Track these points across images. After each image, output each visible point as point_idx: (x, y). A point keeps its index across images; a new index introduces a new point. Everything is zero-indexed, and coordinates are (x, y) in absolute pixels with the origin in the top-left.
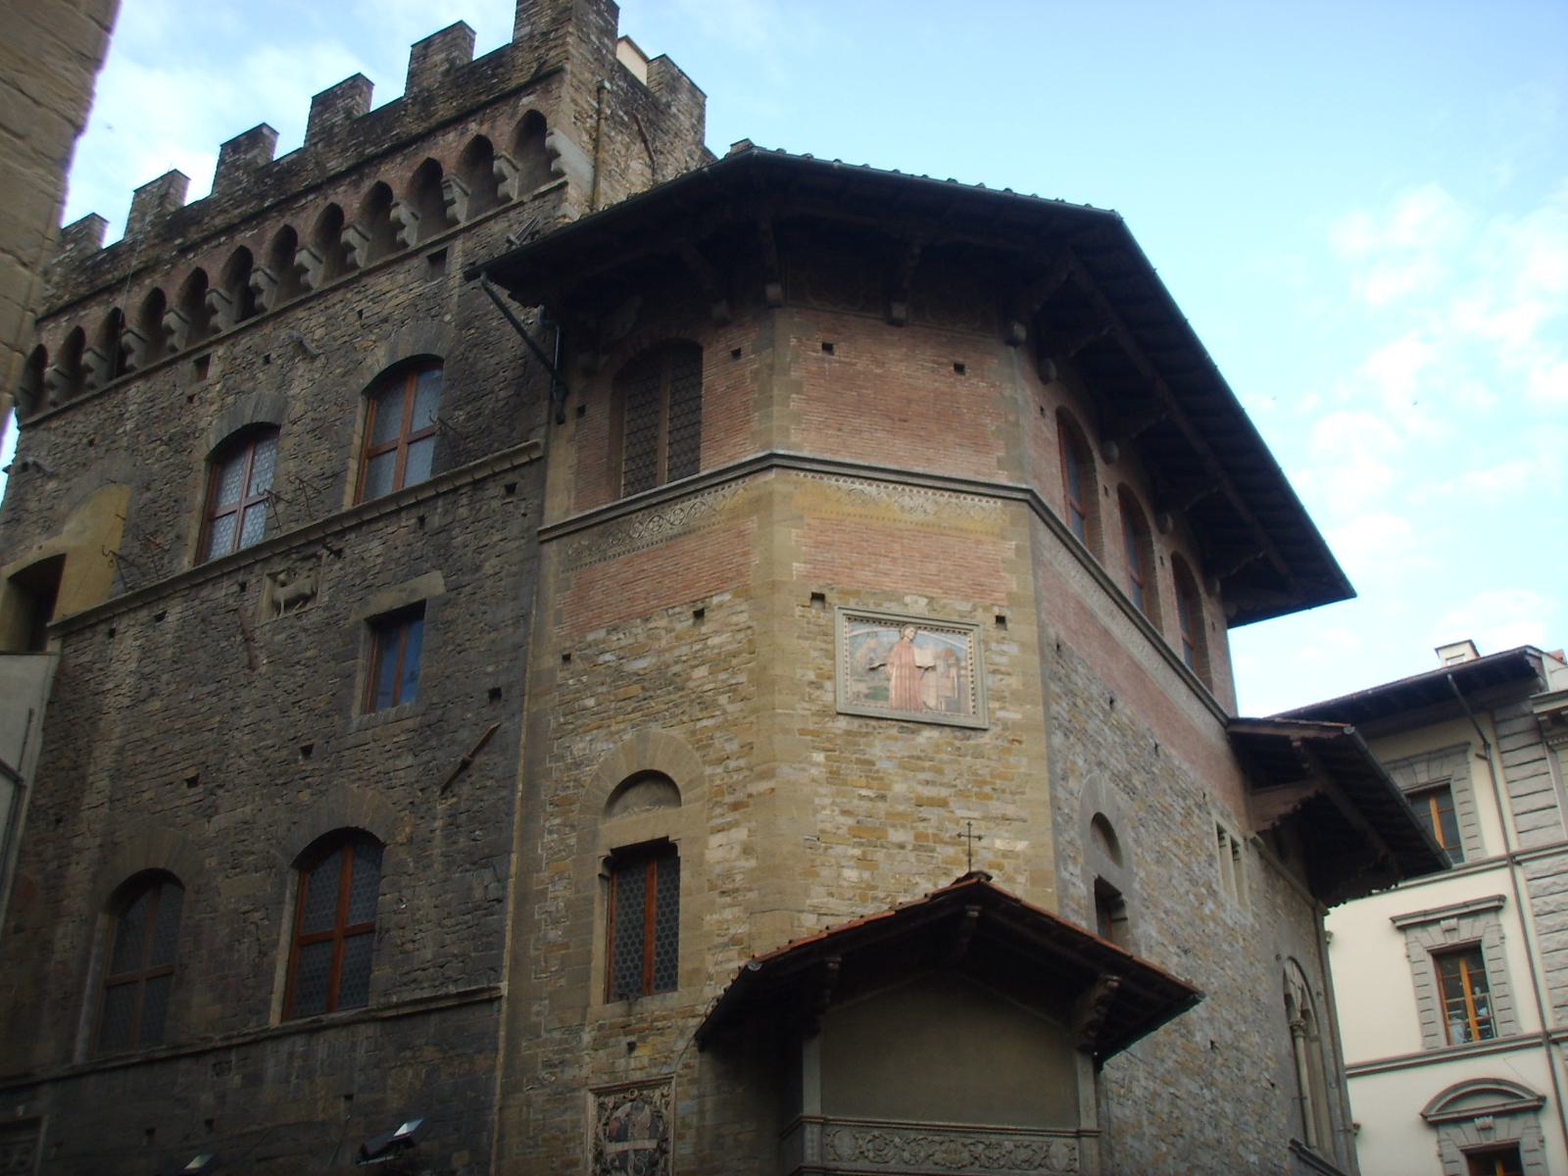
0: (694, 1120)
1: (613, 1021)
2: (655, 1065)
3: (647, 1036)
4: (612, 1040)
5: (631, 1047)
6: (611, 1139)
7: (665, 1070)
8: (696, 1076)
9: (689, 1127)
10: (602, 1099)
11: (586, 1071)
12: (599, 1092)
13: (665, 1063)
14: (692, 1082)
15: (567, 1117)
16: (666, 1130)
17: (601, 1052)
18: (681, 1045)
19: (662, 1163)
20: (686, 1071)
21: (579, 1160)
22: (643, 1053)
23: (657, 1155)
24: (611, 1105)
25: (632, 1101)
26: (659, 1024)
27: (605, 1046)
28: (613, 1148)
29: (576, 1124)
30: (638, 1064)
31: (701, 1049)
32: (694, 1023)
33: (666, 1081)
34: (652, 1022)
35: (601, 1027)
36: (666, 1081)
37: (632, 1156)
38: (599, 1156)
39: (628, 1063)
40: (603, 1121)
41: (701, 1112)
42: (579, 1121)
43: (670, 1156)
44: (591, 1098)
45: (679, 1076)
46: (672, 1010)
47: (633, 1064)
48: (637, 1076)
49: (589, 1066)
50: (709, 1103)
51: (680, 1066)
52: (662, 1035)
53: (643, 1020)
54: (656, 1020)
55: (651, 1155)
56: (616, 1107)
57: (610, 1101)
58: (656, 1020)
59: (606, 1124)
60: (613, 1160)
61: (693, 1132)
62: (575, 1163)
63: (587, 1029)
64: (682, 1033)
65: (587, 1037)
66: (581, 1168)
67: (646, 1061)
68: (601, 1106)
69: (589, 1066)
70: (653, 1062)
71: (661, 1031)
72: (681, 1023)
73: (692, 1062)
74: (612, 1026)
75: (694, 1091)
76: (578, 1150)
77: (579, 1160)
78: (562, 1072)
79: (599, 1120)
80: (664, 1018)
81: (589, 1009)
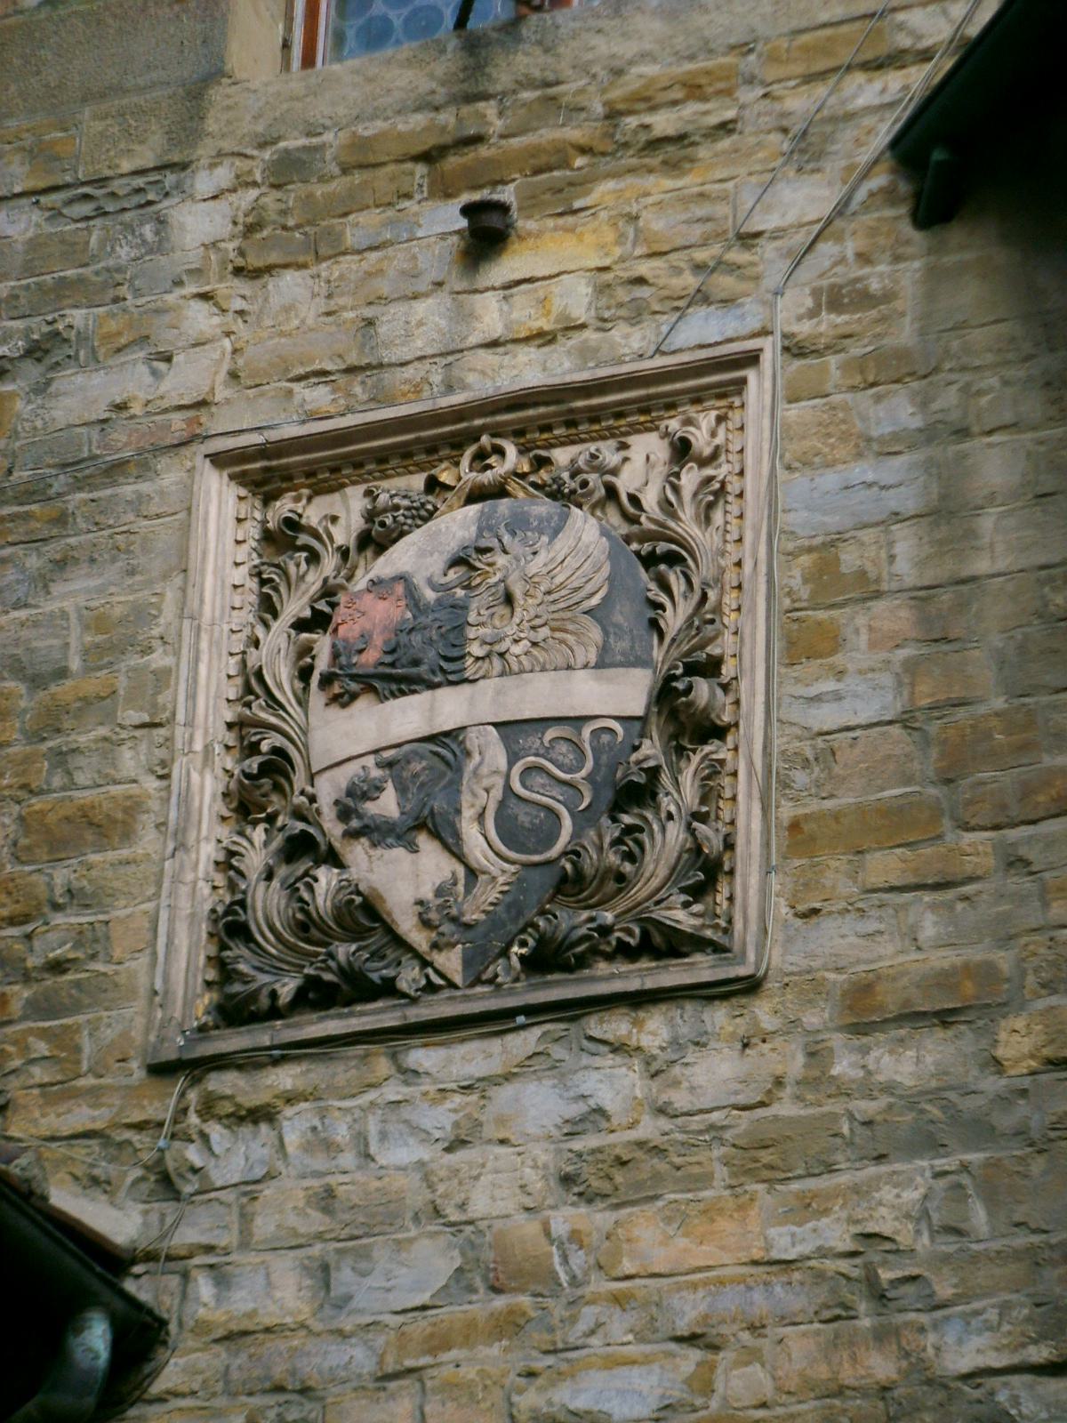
0: (906, 557)
1: (367, 130)
2: (637, 314)
3: (582, 183)
4: (362, 226)
5: (486, 235)
6: (350, 684)
7: (703, 330)
8: (904, 334)
9: (868, 590)
10: (284, 506)
11: (190, 376)
12: (265, 471)
13: (702, 297)
14: (879, 372)
15: (73, 594)
16: (704, 618)
17: (289, 285)
18: (803, 200)
19: (681, 791)
20: (829, 322)
21: (133, 807)
22: (558, 262)
23: (652, 750)
24: (344, 534)
25: (477, 495)
26: (663, 123)
27: (320, 248)
28: (346, 739)
29: (117, 637)
30: (550, 310)
31: (933, 211)
32: (882, 101)
33: (721, 376)
34: (613, 115)
35: (288, 169)
36: (721, 376)
37: (490, 754)
38: (262, 780)
39: (464, 316)
40: (295, 606)
41: (947, 514)
42: (143, 614)
43: (747, 753)
44: (222, 517)
45: (795, 349)
46: (744, 48)
47: (491, 315)
48: (528, 370)
49: (223, 342)
50: (996, 466)
51: (796, 300)
52: (672, 167)
53: (552, 105)
54: (646, 101)
55: (612, 755)
56: (374, 540)
57: (342, 513)
58: (646, 101)
59: (317, 621)
60: (362, 791)
61: (893, 615)
62: (107, 826)
63: (204, 182)
64: (806, 148)
65: (201, 221)
66: (148, 841)
67: (576, 298)
68: (283, 539)
69: (223, 342)
70: (623, 294)
71: (671, 150)
72: (799, 103)
73: (876, 277)
74: (361, 159)
75: (898, 411)
76: (129, 761)
77: (133, 807)
78: (41, 388)
79: (268, 608)
80: (694, 89)
81: (217, 94)
